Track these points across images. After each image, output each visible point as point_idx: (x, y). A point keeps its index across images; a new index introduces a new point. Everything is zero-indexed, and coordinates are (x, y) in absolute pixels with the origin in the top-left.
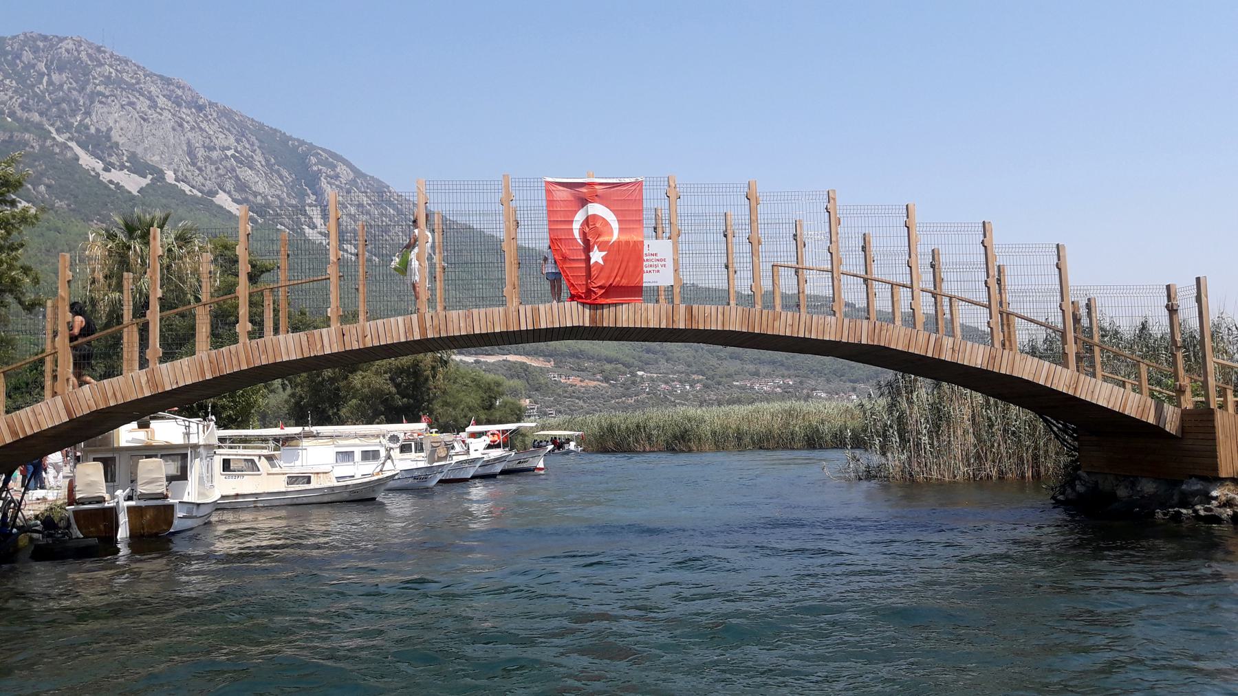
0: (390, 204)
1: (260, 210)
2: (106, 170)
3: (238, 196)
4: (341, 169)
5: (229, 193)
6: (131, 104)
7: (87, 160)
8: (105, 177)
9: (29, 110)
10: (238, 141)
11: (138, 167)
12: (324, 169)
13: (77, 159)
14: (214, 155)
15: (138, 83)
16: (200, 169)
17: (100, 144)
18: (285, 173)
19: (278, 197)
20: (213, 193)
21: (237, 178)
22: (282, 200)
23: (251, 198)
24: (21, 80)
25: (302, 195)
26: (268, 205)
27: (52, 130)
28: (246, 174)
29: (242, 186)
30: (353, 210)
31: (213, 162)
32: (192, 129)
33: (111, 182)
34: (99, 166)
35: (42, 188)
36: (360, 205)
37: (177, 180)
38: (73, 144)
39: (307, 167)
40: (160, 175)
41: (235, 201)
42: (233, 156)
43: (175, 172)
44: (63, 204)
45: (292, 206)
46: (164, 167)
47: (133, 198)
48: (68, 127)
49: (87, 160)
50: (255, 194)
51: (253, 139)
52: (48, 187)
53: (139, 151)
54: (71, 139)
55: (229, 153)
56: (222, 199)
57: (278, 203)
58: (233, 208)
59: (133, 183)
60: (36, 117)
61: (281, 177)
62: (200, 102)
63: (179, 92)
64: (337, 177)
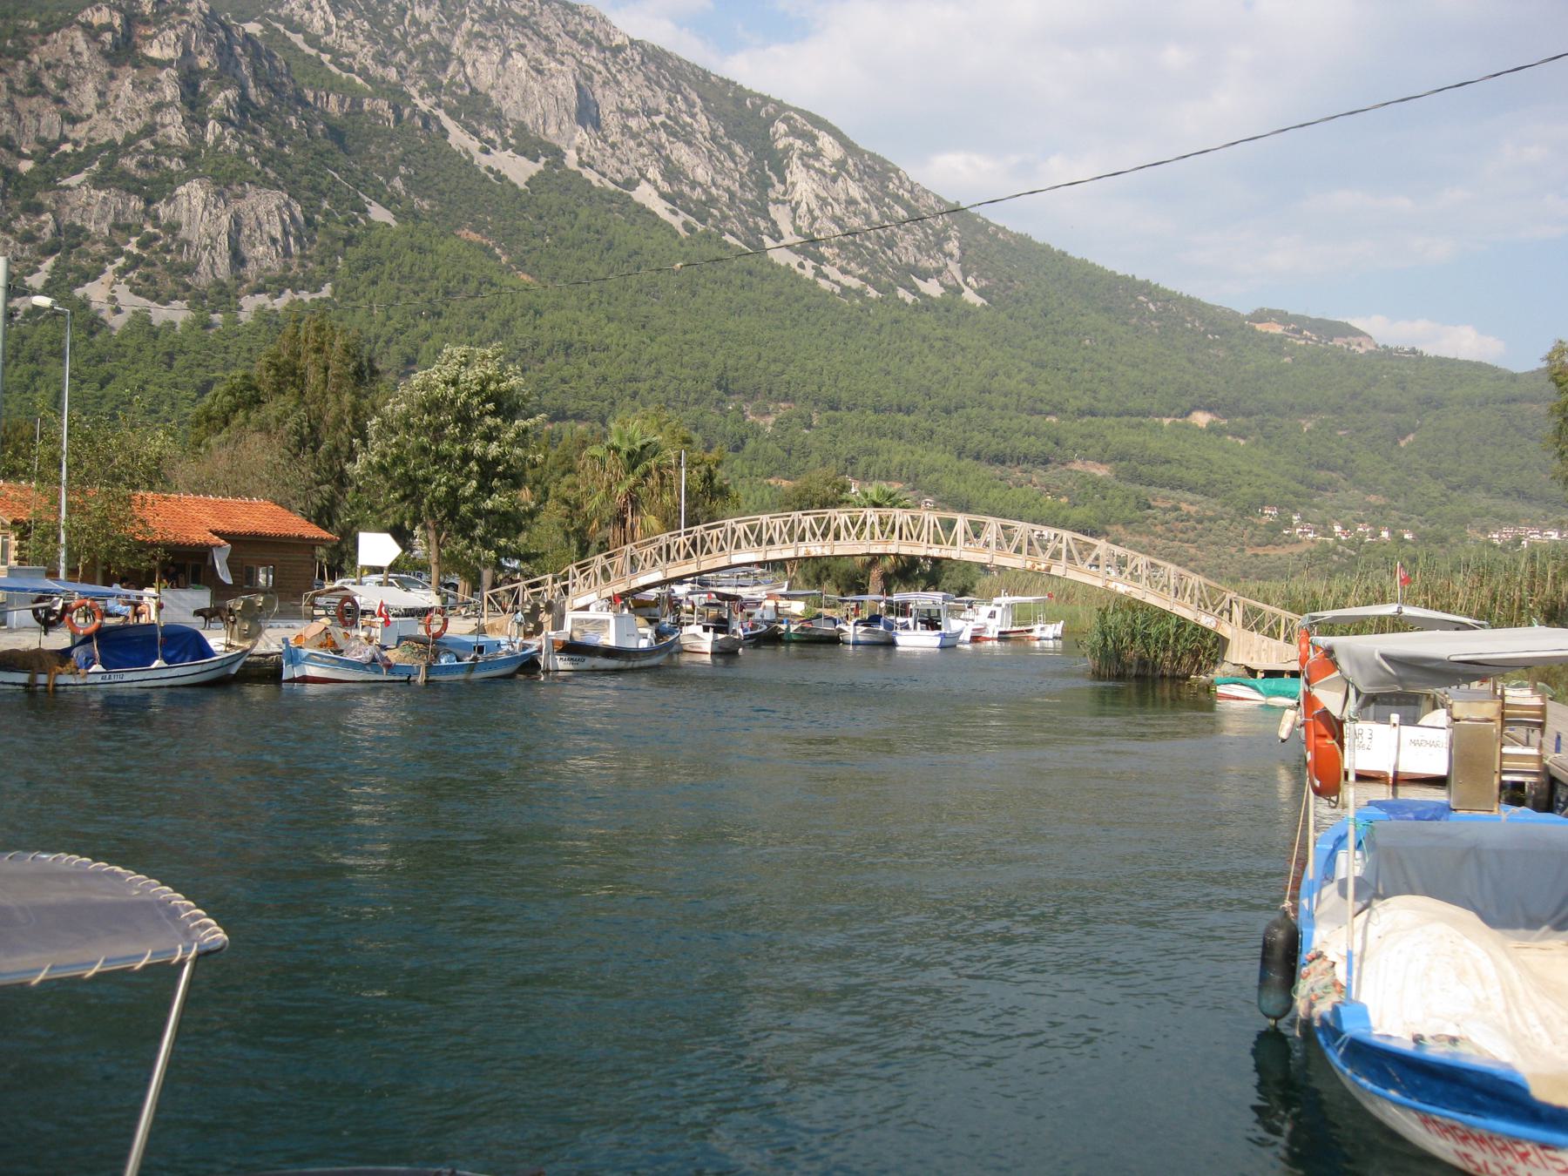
0: (898, 199)
1: (700, 211)
2: (487, 152)
3: (666, 188)
4: (825, 141)
5: (653, 183)
6: (521, 47)
7: (458, 138)
8: (482, 161)
9: (385, 65)
10: (670, 101)
11: (528, 145)
12: (798, 143)
13: (444, 133)
14: (633, 123)
15: (532, 14)
16: (613, 146)
17: (476, 108)
18: (738, 150)
19: (728, 190)
20: (630, 184)
21: (668, 159)
22: (732, 195)
23: (686, 190)
24: (376, 21)
25: (764, 185)
26: (712, 201)
27: (414, 92)
28: (681, 153)
29: (672, 172)
30: (838, 211)
31: (634, 136)
32: (605, 84)
33: (490, 169)
34: (474, 145)
35: (398, 183)
36: (851, 202)
37: (581, 164)
38: (440, 113)
39: (768, 140)
40: (557, 154)
41: (663, 196)
42: (663, 124)
43: (579, 150)
44: (426, 204)
45: (746, 202)
46: (563, 146)
47: (519, 193)
48: (436, 88)
49: (458, 138)
50: (694, 184)
51: (694, 96)
52: (407, 179)
53: (528, 119)
54: (439, 105)
55: (657, 120)
56: (645, 195)
57: (725, 197)
58: (660, 208)
59: (519, 170)
60: (392, 74)
61: (732, 156)
62: (618, 40)
63: (588, 26)
64: (818, 155)
